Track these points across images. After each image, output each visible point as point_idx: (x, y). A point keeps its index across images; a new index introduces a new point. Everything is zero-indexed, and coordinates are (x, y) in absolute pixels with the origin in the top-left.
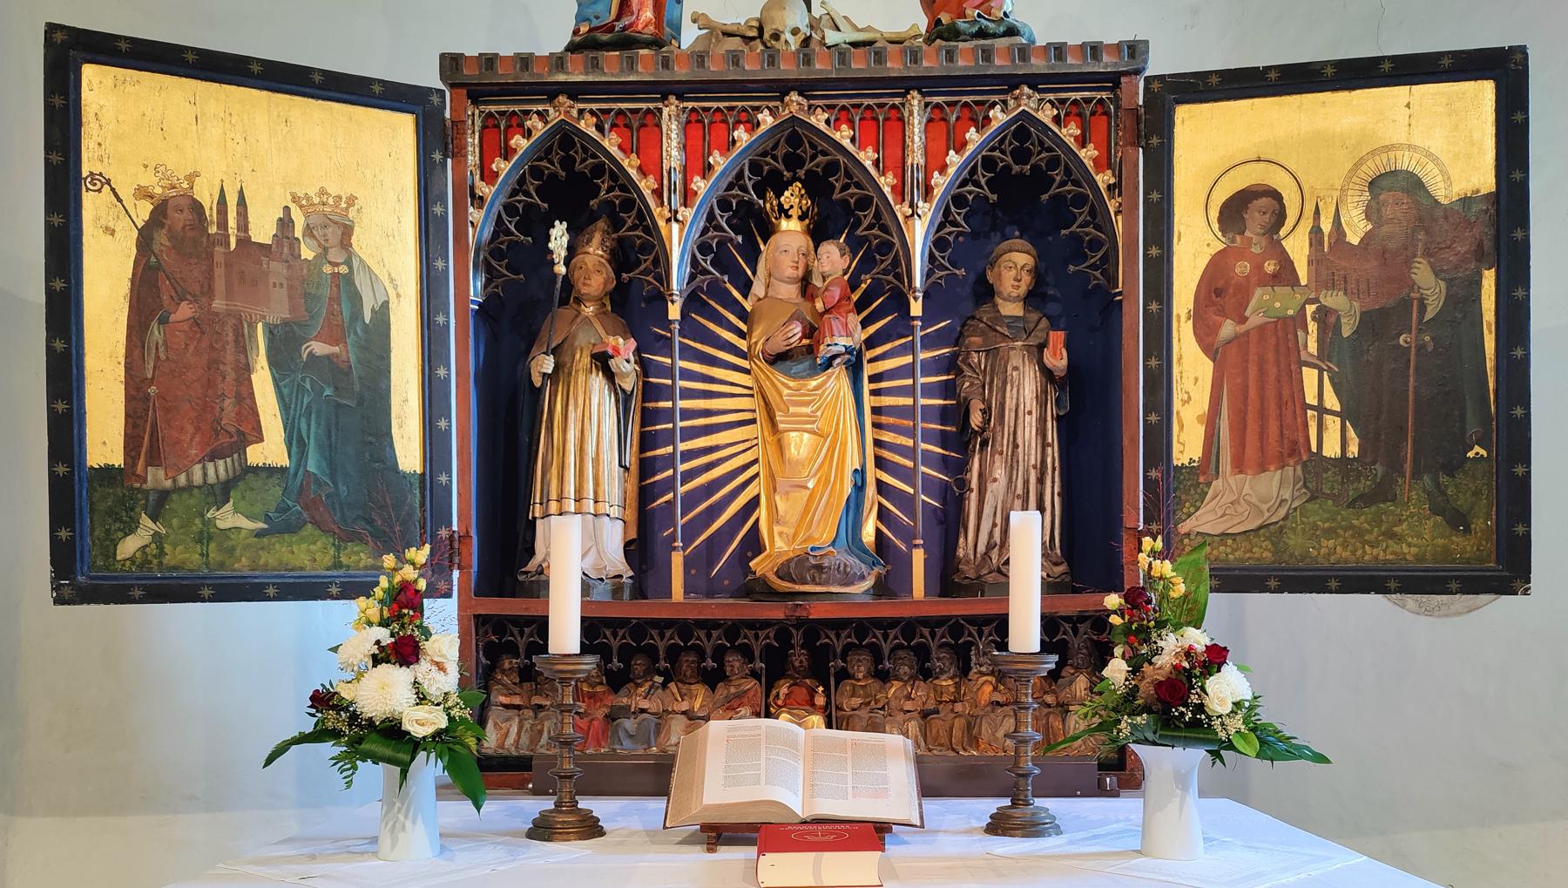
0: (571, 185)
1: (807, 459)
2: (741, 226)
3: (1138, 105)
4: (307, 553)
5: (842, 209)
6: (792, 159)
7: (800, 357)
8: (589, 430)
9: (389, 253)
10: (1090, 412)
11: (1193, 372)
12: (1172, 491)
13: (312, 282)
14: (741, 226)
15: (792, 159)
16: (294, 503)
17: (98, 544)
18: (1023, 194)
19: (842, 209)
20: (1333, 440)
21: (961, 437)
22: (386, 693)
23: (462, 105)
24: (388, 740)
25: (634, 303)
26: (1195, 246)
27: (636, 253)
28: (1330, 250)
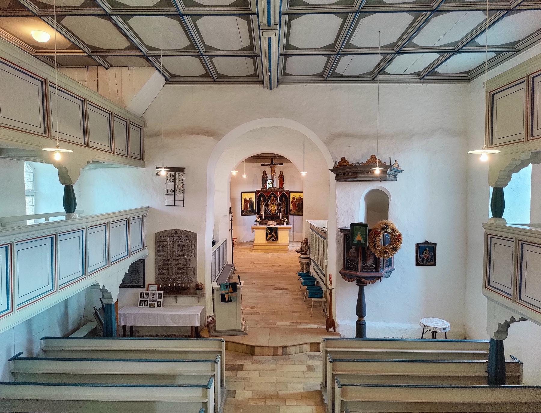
0: (262, 195)
1: (273, 208)
2: (270, 196)
3: (289, 193)
4: (250, 214)
5: (274, 196)
6: (273, 194)
7: (273, 204)
8: (263, 206)
9: (254, 199)
10: (287, 206)
11: (291, 205)
12: (290, 211)
13: (251, 202)
14: (270, 196)
15: (273, 194)
16: (250, 211)
17: (243, 213)
18: (283, 196)
19: (274, 196)
20: (297, 209)
21: (281, 208)
22: (258, 220)
23: (257, 193)
24: (257, 222)
25: (265, 200)
26: (291, 199)
27: (265, 199)
28: (297, 200)
